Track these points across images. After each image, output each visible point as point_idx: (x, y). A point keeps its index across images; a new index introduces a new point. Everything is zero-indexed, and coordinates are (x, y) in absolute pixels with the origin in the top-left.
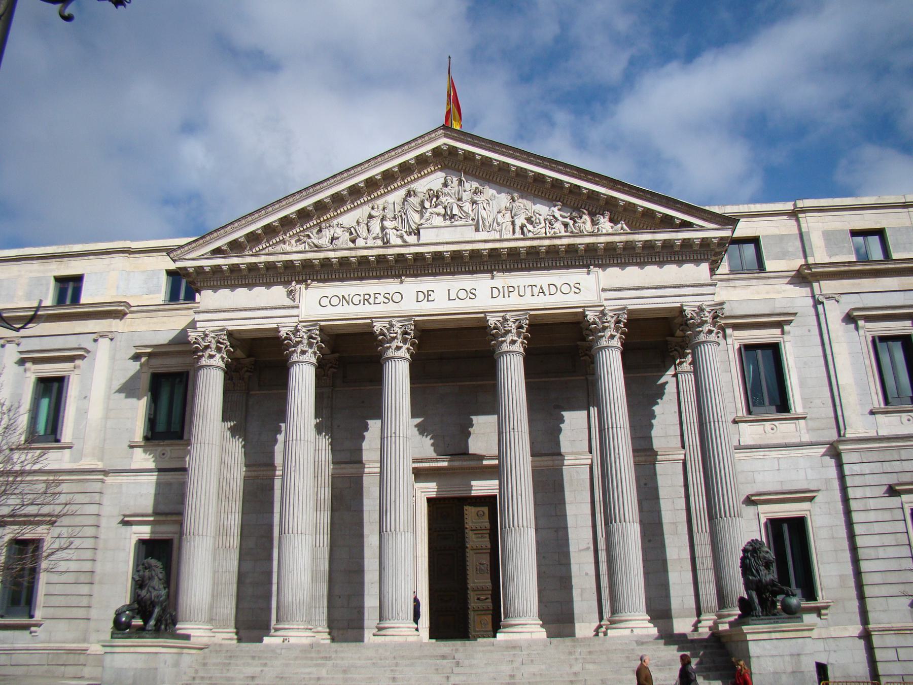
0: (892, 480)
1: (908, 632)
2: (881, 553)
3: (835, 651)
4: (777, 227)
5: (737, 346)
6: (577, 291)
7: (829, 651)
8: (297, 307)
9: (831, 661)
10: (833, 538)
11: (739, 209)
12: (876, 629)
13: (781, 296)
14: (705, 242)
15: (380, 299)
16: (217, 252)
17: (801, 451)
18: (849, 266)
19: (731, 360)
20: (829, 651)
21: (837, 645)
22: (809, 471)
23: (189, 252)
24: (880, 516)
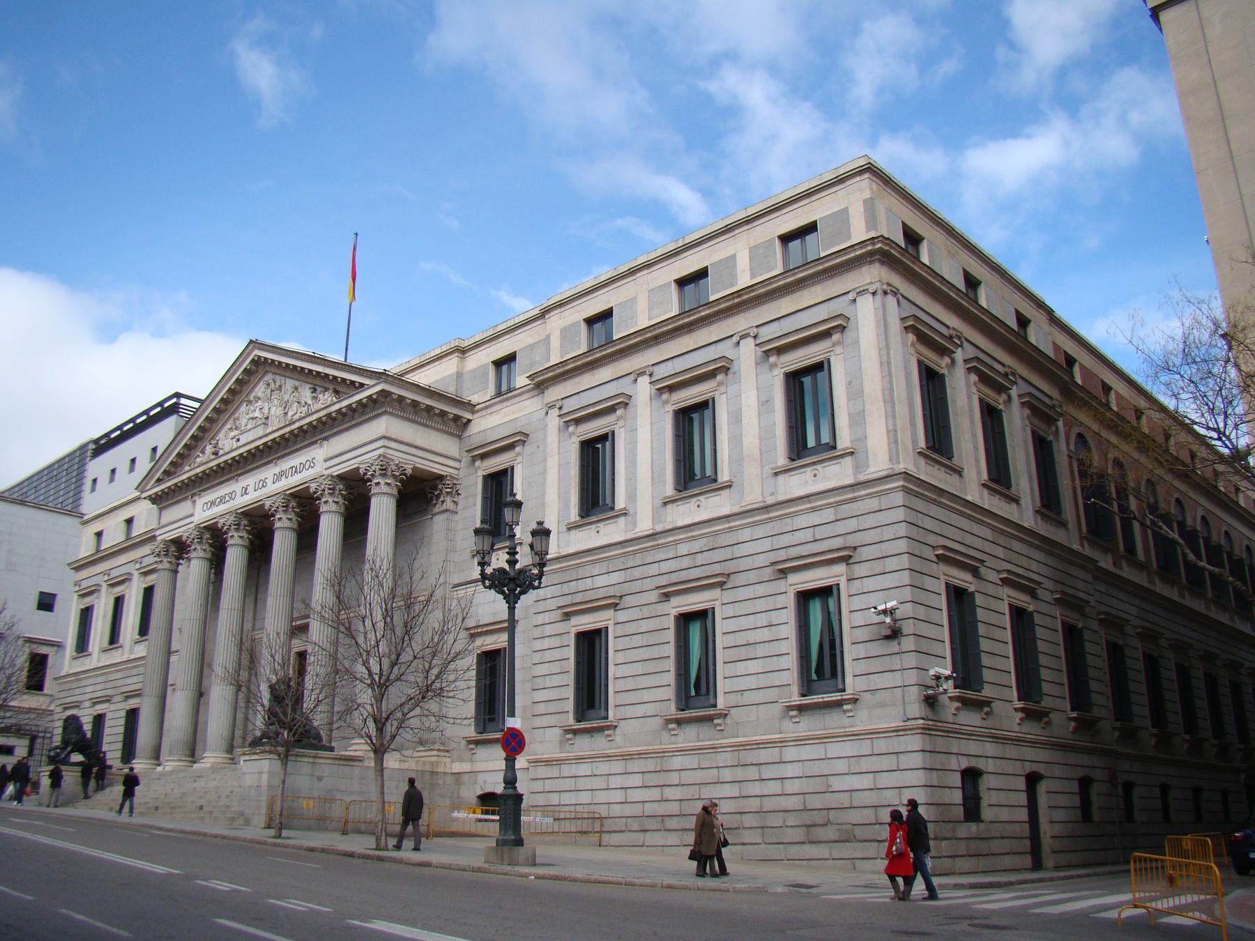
0: (568, 600)
2: (548, 682)
4: (531, 336)
6: (312, 465)
8: (192, 515)
10: (523, 668)
13: (523, 413)
15: (227, 498)
16: (159, 480)
18: (563, 366)
23: (146, 485)
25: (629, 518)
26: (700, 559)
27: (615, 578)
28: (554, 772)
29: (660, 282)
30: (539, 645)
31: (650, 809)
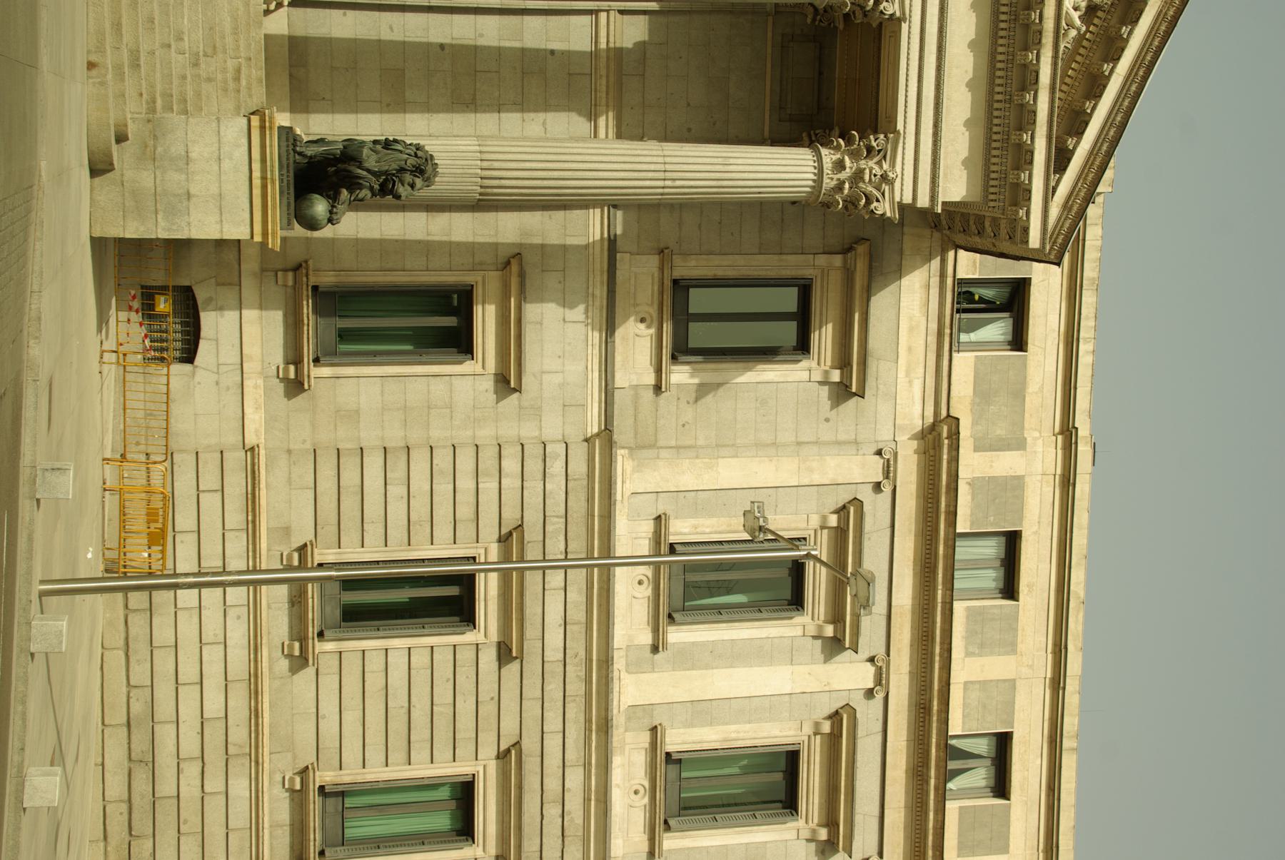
1: (250, 518)
2: (397, 491)
3: (217, 383)
4: (1042, 387)
5: (808, 273)
7: (218, 373)
9: (200, 375)
10: (429, 407)
11: (1087, 318)
12: (256, 461)
13: (901, 374)
14: (1021, 195)
17: (596, 367)
18: (947, 513)
19: (784, 257)
20: (218, 373)
21: (228, 388)
22: (557, 379)
24: (466, 499)
25: (647, 653)
26: (553, 811)
27: (554, 638)
28: (236, 518)
29: (1021, 700)
30: (466, 462)
31: (166, 734)
